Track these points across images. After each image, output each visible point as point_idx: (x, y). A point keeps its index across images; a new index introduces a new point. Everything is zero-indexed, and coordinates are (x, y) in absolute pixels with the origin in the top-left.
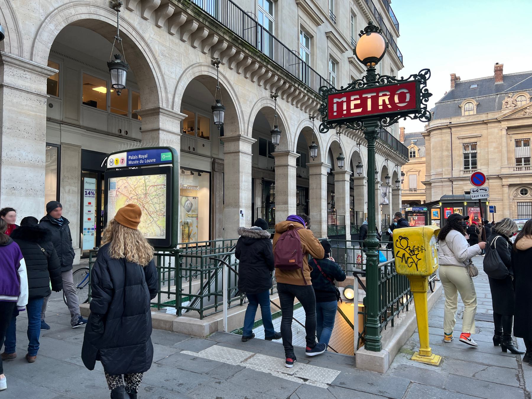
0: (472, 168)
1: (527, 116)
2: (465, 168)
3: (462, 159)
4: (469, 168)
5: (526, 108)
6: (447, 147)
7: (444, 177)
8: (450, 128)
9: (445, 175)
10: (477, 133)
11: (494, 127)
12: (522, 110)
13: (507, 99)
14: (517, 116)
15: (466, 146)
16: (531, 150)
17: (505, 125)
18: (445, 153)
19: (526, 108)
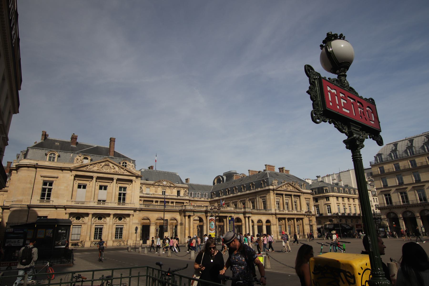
0: (47, 199)
1: (88, 170)
2: (41, 199)
3: (117, 196)
4: (44, 199)
5: (88, 165)
6: (31, 181)
7: (23, 204)
8: (36, 168)
9: (25, 202)
10: (55, 175)
11: (67, 173)
12: (85, 166)
13: (78, 157)
14: (82, 169)
15: (45, 183)
16: (108, 193)
17: (74, 173)
18: (29, 186)
19: (88, 165)
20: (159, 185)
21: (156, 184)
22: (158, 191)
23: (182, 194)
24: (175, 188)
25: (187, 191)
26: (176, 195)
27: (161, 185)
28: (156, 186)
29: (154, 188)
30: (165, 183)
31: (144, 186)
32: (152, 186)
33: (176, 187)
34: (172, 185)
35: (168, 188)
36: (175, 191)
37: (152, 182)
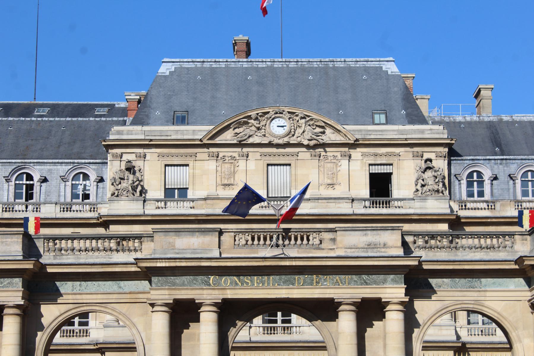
20: (240, 145)
21: (228, 137)
23: (402, 186)
24: (357, 153)
25: (441, 164)
26: (365, 192)
28: (223, 152)
29: (212, 165)
30: (278, 128)
31: (151, 153)
32: (203, 153)
33: (355, 145)
34: (330, 136)
35: (305, 154)
36: (352, 177)
37: (198, 131)
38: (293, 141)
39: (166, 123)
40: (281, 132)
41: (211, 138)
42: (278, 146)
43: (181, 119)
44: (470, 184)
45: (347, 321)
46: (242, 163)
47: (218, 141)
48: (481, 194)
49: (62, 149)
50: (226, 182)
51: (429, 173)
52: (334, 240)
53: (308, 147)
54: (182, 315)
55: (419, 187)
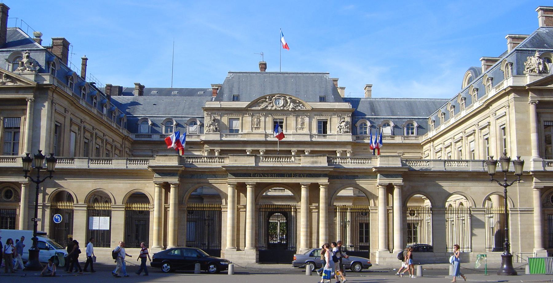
22: (262, 124)
27: (269, 108)
37: (243, 104)
38: (285, 108)
39: (229, 100)
40: (281, 105)
41: (250, 107)
42: (278, 110)
43: (236, 98)
44: (361, 128)
45: (304, 192)
46: (262, 119)
47: (254, 108)
48: (366, 133)
49: (185, 111)
50: (255, 126)
51: (343, 124)
52: (300, 160)
53: (291, 111)
54: (241, 188)
55: (338, 129)
